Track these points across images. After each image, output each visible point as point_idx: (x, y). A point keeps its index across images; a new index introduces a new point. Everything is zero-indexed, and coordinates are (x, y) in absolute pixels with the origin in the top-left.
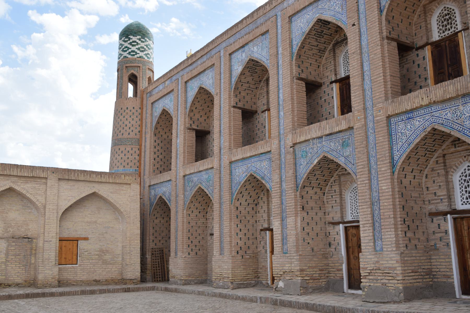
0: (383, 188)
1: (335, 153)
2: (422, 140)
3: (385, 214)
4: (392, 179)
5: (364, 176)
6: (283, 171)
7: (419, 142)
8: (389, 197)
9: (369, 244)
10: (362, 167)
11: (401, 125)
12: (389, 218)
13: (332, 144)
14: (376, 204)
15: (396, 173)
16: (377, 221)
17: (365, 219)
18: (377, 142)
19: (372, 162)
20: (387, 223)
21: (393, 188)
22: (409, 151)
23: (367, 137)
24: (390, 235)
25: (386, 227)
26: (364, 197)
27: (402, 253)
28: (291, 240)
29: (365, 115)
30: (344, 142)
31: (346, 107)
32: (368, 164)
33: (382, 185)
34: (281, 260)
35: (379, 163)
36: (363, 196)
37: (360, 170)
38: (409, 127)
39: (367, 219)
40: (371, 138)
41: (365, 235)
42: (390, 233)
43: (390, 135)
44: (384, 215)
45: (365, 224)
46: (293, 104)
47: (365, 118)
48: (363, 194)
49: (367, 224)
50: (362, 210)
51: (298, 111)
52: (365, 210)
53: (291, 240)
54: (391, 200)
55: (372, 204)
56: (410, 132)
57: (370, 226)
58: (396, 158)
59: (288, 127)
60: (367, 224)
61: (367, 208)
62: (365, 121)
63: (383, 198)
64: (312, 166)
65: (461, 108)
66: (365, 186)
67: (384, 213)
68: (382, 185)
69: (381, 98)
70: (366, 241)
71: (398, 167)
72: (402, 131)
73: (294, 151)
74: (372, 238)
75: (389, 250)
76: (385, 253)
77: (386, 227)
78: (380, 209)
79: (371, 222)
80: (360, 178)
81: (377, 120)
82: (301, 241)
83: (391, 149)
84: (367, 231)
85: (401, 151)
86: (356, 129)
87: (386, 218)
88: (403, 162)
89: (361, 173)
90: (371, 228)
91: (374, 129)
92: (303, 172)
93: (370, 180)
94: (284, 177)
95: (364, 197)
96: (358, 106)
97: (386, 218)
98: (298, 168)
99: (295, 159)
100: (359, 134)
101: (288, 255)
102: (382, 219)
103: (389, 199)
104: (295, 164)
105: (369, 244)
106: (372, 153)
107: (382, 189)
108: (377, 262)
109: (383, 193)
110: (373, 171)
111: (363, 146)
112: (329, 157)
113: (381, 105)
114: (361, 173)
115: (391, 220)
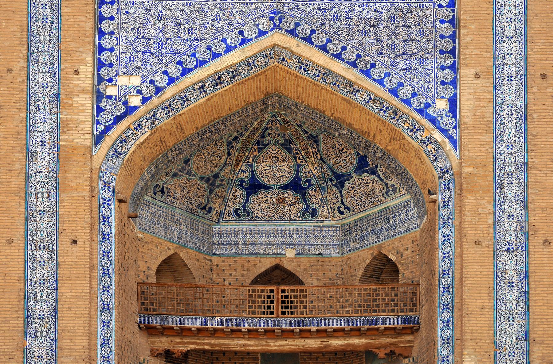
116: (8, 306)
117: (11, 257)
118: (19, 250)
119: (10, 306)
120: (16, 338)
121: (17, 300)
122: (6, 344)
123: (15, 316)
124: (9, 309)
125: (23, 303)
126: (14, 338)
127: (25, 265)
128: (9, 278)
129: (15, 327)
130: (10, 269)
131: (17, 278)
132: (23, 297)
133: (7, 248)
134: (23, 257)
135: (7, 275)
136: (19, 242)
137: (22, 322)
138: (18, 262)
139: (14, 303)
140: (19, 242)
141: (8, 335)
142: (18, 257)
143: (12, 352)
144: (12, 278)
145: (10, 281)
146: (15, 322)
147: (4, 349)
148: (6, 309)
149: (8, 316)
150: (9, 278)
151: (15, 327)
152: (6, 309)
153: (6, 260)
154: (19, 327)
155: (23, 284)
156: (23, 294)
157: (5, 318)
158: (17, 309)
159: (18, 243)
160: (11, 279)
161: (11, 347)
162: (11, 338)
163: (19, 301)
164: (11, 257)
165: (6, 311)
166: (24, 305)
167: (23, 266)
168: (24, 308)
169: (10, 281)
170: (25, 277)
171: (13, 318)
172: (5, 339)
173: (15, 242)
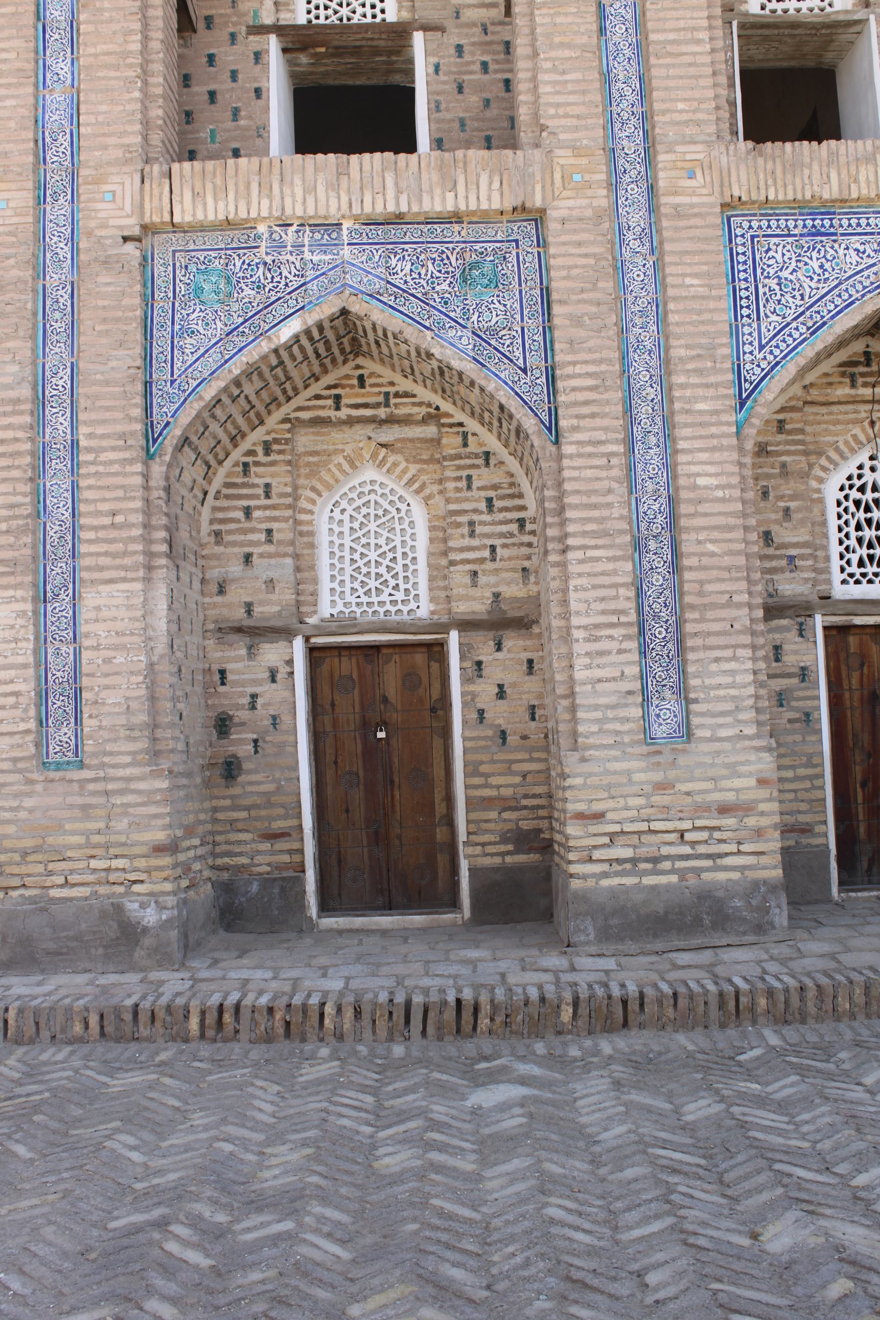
0: (701, 481)
1: (414, 307)
3: (709, 588)
5: (598, 422)
9: (622, 713)
10: (590, 382)
12: (730, 604)
14: (652, 545)
16: (656, 617)
17: (600, 606)
24: (733, 673)
25: (712, 641)
26: (596, 513)
28: (112, 697)
30: (474, 266)
33: (695, 469)
34: (28, 803)
36: (595, 506)
37: (581, 396)
38: (815, 265)
39: (612, 605)
41: (599, 673)
42: (733, 665)
44: (701, 594)
45: (597, 626)
47: (614, 186)
48: (594, 499)
49: (612, 625)
50: (586, 568)
52: (600, 567)
53: (112, 697)
55: (638, 545)
57: (627, 637)
59: (112, 141)
60: (612, 625)
66: (609, 467)
67: (701, 583)
68: (695, 469)
69: (698, 123)
70: (603, 701)
72: (785, 274)
75: (723, 733)
76: (704, 747)
77: (712, 641)
79: (633, 617)
80: (575, 429)
81: (676, 207)
84: (613, 658)
87: (714, 606)
89: (585, 410)
90: (633, 645)
95: (596, 513)
96: (576, 129)
97: (714, 606)
100: (579, 244)
101: (86, 774)
102: (692, 607)
103: (729, 528)
105: (622, 713)
107: (695, 487)
108: (662, 787)
113: (697, 152)
114: (585, 410)
115: (734, 613)
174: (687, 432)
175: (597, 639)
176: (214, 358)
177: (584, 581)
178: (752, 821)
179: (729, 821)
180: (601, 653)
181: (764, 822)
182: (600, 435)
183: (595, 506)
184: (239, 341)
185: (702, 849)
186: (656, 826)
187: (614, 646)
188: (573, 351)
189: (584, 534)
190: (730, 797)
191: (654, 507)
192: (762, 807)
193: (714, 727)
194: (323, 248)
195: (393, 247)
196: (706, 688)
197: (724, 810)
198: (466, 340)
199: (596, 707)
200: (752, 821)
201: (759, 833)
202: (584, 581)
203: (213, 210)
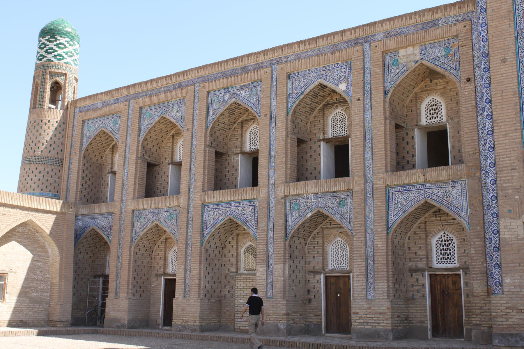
0: (379, 246)
1: (330, 210)
2: (415, 209)
3: (379, 268)
4: (387, 239)
5: (360, 234)
6: (271, 220)
7: (413, 211)
8: (384, 254)
9: (362, 293)
11: (398, 195)
12: (383, 271)
13: (328, 202)
14: (370, 258)
15: (390, 234)
18: (375, 206)
19: (369, 221)
20: (380, 276)
21: (387, 247)
22: (403, 217)
23: (365, 201)
24: (383, 285)
25: (379, 279)
27: (392, 301)
29: (364, 181)
30: (341, 201)
31: (341, 168)
32: (365, 224)
33: (377, 243)
35: (376, 224)
36: (359, 251)
37: (357, 228)
39: (361, 271)
40: (369, 202)
41: (358, 284)
42: (383, 284)
43: (387, 202)
44: (378, 269)
45: (358, 275)
46: (286, 157)
47: (365, 183)
50: (357, 263)
51: (291, 164)
54: (385, 257)
55: (367, 258)
56: (405, 202)
58: (391, 222)
59: (280, 179)
61: (362, 262)
62: (364, 186)
63: (377, 254)
64: (305, 218)
65: (450, 189)
66: (361, 243)
67: (378, 267)
68: (377, 243)
71: (393, 230)
72: (399, 200)
73: (286, 202)
74: (365, 287)
75: (381, 298)
76: (377, 300)
77: (379, 279)
78: (374, 263)
79: (365, 273)
80: (356, 235)
81: (376, 187)
82: (287, 287)
83: (387, 213)
84: (361, 282)
85: (397, 216)
86: (355, 192)
87: (380, 272)
88: (397, 226)
89: (358, 231)
90: (365, 279)
91: (372, 193)
92: (295, 223)
93: (366, 237)
94: (272, 226)
97: (380, 272)
98: (288, 219)
99: (286, 210)
100: (358, 197)
103: (383, 255)
104: (286, 215)
105: (362, 293)
106: (370, 214)
107: (377, 247)
108: (369, 308)
109: (378, 250)
110: (369, 231)
111: (361, 207)
112: (324, 212)
114: (358, 231)
116: (507, 120)
117: (506, 75)
118: (512, 67)
119: (509, 120)
120: (516, 149)
121: (514, 113)
122: (508, 156)
123: (513, 128)
124: (508, 123)
125: (519, 115)
126: (514, 149)
127: (518, 80)
128: (506, 94)
129: (514, 139)
130: (506, 85)
131: (512, 93)
132: (519, 109)
133: (502, 67)
134: (516, 73)
135: (504, 91)
136: (512, 60)
137: (520, 133)
138: (512, 78)
139: (512, 116)
140: (512, 60)
141: (509, 147)
142: (512, 74)
143: (514, 163)
144: (508, 94)
145: (507, 97)
146: (514, 134)
147: (507, 161)
148: (506, 123)
149: (508, 129)
150: (506, 94)
151: (514, 139)
152: (506, 123)
153: (502, 78)
154: (517, 138)
155: (518, 98)
156: (519, 107)
157: (505, 131)
158: (515, 122)
159: (511, 61)
160: (507, 95)
161: (512, 158)
162: (512, 149)
163: (516, 114)
164: (506, 75)
165: (505, 125)
166: (520, 117)
167: (517, 81)
168: (520, 120)
169: (507, 97)
170: (519, 90)
171: (512, 130)
172: (506, 152)
173: (508, 60)
174: (376, 235)
175: (358, 278)
176: (296, 221)
177: (356, 266)
178: (386, 316)
179: (382, 316)
180: (359, 280)
181: (388, 317)
182: (360, 236)
183: (359, 251)
184: (301, 218)
185: (376, 321)
186: (368, 316)
187: (361, 279)
188: (356, 219)
189: (357, 256)
190: (382, 311)
191: (370, 250)
192: (388, 313)
193: (379, 296)
194: (315, 198)
195: (327, 198)
196: (377, 288)
197: (380, 314)
198: (339, 217)
199: (357, 291)
200: (386, 316)
201: (387, 319)
202: (356, 266)
203: (296, 192)
